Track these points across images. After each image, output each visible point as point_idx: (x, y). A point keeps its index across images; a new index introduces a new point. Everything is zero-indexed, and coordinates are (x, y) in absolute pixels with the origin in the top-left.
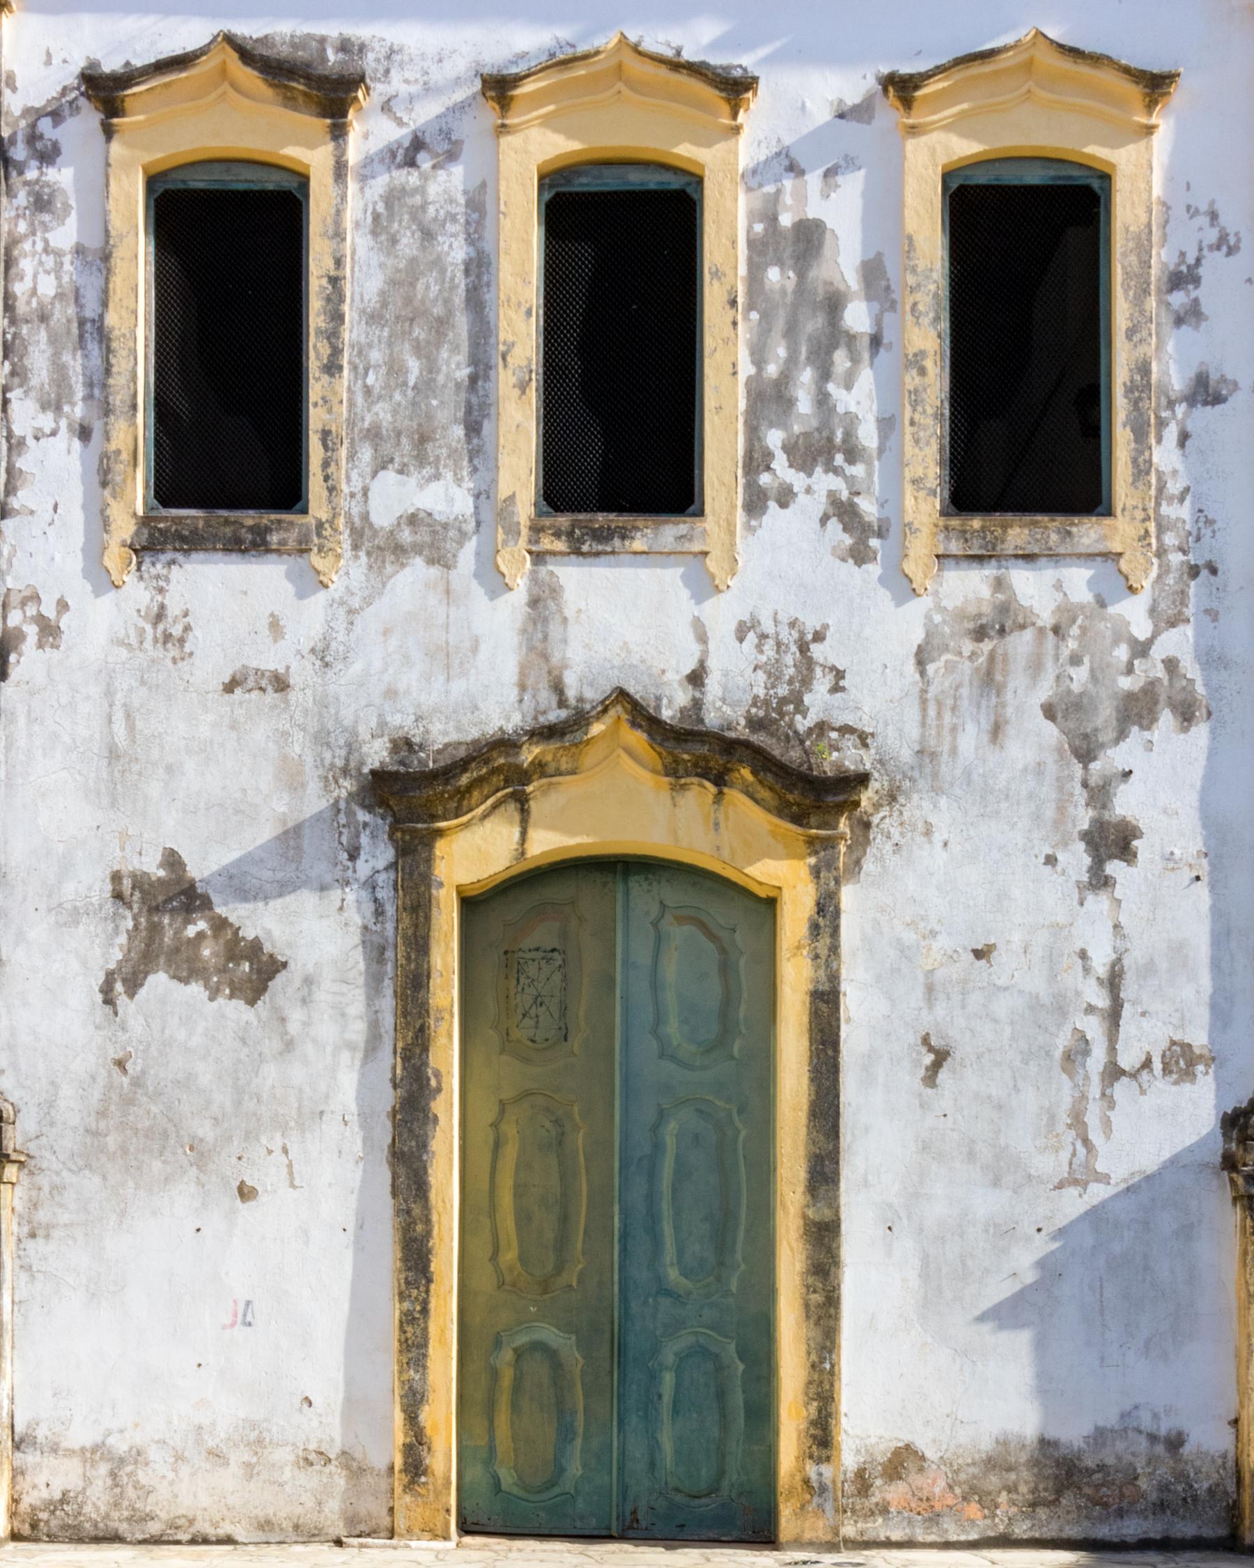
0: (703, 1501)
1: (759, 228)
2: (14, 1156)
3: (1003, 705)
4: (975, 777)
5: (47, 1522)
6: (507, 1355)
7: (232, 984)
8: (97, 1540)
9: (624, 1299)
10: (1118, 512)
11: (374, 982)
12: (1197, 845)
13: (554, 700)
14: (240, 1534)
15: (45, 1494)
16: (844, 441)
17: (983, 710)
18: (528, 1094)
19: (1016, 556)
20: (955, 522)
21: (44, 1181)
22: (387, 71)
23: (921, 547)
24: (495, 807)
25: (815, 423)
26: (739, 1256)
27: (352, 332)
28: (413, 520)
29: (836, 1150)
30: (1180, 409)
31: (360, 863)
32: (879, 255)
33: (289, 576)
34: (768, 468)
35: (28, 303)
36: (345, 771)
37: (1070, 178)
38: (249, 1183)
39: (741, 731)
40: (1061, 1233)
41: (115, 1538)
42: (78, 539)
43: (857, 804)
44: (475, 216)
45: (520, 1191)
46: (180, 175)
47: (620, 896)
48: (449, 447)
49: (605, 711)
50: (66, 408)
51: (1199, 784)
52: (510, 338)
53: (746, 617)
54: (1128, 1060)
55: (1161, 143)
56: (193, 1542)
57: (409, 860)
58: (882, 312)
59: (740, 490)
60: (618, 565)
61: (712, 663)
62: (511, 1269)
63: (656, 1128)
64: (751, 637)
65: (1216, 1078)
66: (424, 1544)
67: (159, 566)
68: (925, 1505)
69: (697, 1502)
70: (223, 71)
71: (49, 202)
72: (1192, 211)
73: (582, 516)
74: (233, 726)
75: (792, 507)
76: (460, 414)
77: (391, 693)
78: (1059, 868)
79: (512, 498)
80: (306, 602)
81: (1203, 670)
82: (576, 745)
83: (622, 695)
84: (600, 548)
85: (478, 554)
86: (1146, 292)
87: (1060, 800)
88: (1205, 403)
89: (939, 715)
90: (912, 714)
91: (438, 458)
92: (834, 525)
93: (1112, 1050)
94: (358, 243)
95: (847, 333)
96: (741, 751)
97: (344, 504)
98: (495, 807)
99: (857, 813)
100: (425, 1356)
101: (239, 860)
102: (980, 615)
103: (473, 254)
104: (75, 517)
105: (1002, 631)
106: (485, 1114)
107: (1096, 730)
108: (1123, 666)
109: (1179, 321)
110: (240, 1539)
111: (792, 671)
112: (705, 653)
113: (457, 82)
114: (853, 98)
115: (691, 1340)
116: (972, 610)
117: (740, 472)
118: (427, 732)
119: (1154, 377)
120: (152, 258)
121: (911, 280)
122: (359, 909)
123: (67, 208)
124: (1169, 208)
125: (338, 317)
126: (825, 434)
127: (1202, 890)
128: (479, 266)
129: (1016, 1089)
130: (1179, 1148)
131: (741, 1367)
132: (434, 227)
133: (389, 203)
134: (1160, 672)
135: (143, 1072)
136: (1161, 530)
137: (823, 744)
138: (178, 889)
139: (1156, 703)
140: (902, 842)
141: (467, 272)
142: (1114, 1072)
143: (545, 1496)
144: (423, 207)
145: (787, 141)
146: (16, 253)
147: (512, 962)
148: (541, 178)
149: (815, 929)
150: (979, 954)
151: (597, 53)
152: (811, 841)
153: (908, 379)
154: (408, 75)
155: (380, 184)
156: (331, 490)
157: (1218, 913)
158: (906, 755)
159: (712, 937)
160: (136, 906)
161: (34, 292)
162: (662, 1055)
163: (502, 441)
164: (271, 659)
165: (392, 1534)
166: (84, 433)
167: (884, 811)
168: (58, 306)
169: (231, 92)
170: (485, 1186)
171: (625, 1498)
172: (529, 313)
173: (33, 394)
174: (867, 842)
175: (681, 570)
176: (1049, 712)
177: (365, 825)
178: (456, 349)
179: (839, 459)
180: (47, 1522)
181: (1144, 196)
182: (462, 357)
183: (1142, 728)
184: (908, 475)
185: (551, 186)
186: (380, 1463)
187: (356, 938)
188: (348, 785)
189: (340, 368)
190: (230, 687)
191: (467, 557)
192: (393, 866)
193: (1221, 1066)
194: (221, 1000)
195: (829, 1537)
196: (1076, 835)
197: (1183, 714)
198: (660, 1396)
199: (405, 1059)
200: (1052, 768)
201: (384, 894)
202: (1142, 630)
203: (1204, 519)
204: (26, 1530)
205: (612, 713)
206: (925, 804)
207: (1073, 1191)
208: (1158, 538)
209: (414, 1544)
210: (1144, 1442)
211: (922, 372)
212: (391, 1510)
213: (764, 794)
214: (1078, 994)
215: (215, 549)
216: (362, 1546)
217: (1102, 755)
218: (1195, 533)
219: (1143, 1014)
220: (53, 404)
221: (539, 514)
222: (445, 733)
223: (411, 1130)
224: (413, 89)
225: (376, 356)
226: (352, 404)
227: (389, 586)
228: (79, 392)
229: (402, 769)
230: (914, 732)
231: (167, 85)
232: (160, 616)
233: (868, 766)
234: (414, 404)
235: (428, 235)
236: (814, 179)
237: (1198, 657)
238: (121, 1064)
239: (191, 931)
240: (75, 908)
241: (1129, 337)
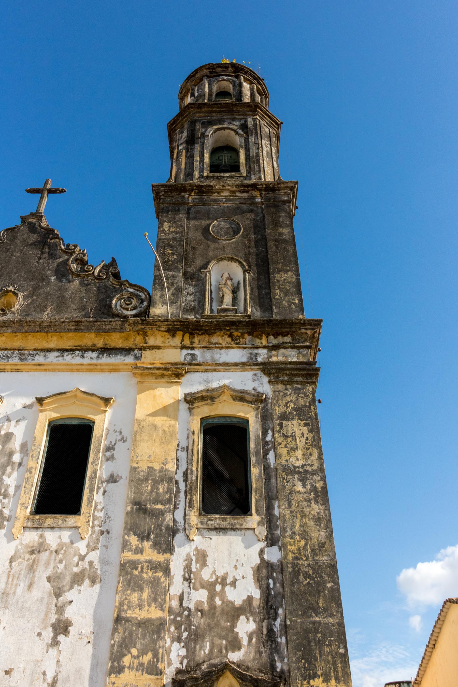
4: (20, 602)
17: (27, 579)
51: (94, 606)
72: (115, 431)
81: (100, 565)
87: (47, 611)
108: (75, 564)
124: (109, 430)
127: (90, 646)
134: (87, 566)
136: (94, 519)
139: (84, 576)
176: (49, 579)
181: (102, 427)
183: (79, 585)
197: (92, 580)
200: (46, 599)
202: (83, 551)
203: (107, 516)
208: (93, 522)
217: (63, 595)
218: (104, 521)
237: (99, 561)
241: (92, 464)
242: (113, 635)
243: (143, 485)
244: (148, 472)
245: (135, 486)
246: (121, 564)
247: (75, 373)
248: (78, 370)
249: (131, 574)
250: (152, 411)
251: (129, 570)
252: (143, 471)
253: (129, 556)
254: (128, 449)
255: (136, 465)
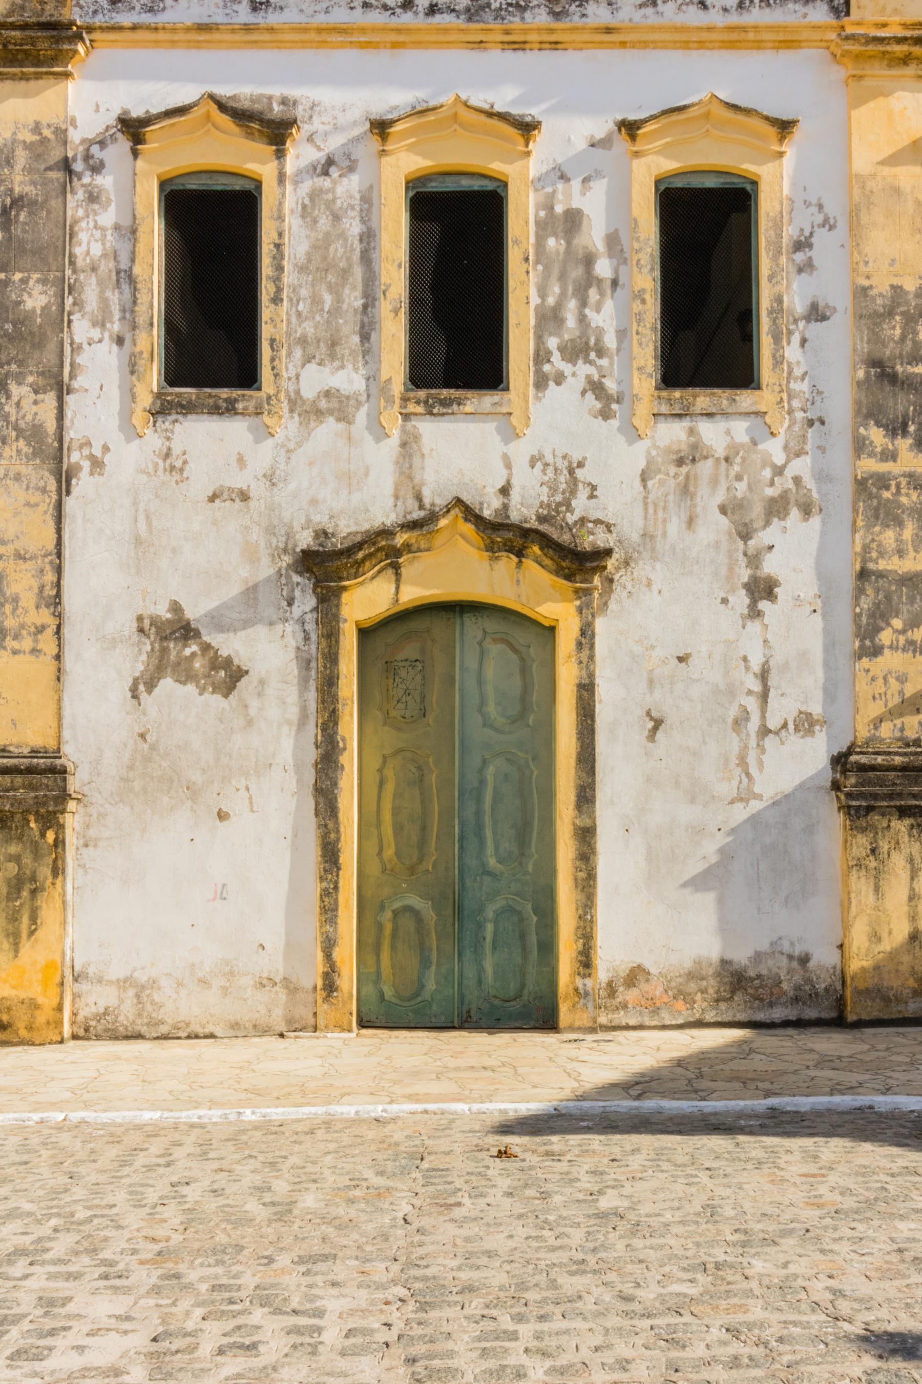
0: (512, 1003)
1: (542, 214)
2: (74, 796)
3: (695, 506)
5: (95, 1027)
6: (388, 914)
7: (213, 684)
8: (127, 1038)
9: (462, 877)
10: (764, 387)
11: (304, 682)
12: (816, 590)
13: (416, 505)
14: (218, 1032)
15: (94, 1009)
16: (596, 344)
18: (400, 751)
19: (702, 414)
20: (664, 394)
21: (93, 810)
22: (311, 117)
23: (644, 409)
24: (379, 572)
25: (577, 333)
26: (533, 850)
27: (289, 277)
28: (327, 394)
29: (594, 782)
30: (802, 324)
31: (294, 608)
32: (616, 230)
33: (249, 429)
34: (549, 361)
35: (84, 260)
36: (285, 551)
37: (733, 183)
38: (224, 809)
39: (533, 524)
40: (733, 831)
41: (139, 1036)
42: (116, 406)
43: (605, 568)
44: (366, 206)
45: (396, 811)
46: (181, 181)
47: (458, 627)
48: (350, 349)
49: (448, 511)
50: (108, 325)
51: (815, 553)
52: (388, 282)
53: (536, 453)
54: (773, 723)
55: (788, 162)
56: (189, 1037)
57: (325, 605)
58: (618, 265)
59: (532, 374)
60: (456, 421)
61: (515, 482)
62: (390, 861)
63: (481, 771)
64: (539, 465)
65: (827, 734)
66: (336, 1035)
67: (167, 423)
68: (650, 1002)
69: (508, 1004)
70: (208, 116)
71: (98, 197)
73: (433, 391)
74: (214, 523)
75: (564, 385)
76: (357, 329)
77: (314, 502)
78: (730, 606)
79: (390, 380)
80: (260, 445)
82: (430, 533)
83: (459, 501)
84: (445, 411)
85: (368, 415)
86: (780, 253)
88: (817, 320)
89: (655, 512)
90: (639, 511)
91: (343, 356)
92: (590, 396)
93: (763, 717)
94: (293, 223)
95: (597, 278)
96: (533, 536)
97: (284, 384)
98: (379, 572)
99: (605, 573)
100: (336, 916)
101: (218, 607)
102: (680, 451)
103: (365, 230)
104: (114, 393)
105: (694, 460)
106: (374, 763)
107: (752, 520)
108: (768, 481)
109: (800, 270)
110: (218, 1035)
111: (564, 486)
112: (510, 475)
113: (355, 123)
114: (600, 135)
115: (504, 903)
116: (675, 448)
117: (531, 363)
118: (337, 525)
119: (785, 305)
120: (163, 232)
121: (636, 245)
122: (294, 637)
123: (109, 201)
125: (280, 269)
126: (584, 340)
127: (817, 617)
128: (369, 237)
129: (704, 742)
130: (805, 778)
131: (535, 919)
132: (340, 213)
133: (312, 199)
134: (790, 485)
135: (157, 741)
136: (790, 398)
137: (584, 531)
138: (179, 625)
139: (788, 504)
140: (633, 590)
141: (361, 240)
142: (765, 731)
143: (413, 1003)
144: (334, 201)
145: (560, 160)
146: (76, 229)
147: (390, 669)
148: (407, 183)
149: (580, 645)
150: (681, 659)
151: (442, 106)
152: (577, 591)
153: (634, 306)
154: (323, 119)
155: (306, 186)
156: (276, 375)
157: (827, 632)
158: (635, 537)
159: (516, 651)
160: (152, 637)
161: (88, 253)
162: (484, 725)
163: (383, 345)
164: (238, 481)
165: (315, 1029)
166: (120, 341)
167: (622, 572)
168: (103, 262)
169: (213, 130)
170: (374, 809)
171: (462, 1003)
172: (400, 266)
173: (87, 317)
174: (611, 591)
175: (495, 424)
176: (723, 510)
177: (298, 584)
178: (354, 288)
179: (593, 355)
180: (95, 1027)
182: (358, 293)
183: (780, 519)
184: (635, 365)
185: (413, 188)
186: (308, 985)
187: (292, 655)
188: (287, 559)
189: (282, 300)
190: (212, 499)
191: (361, 416)
192: (316, 609)
193: (830, 726)
194: (206, 695)
195: (590, 1024)
196: (740, 586)
197: (805, 510)
198: (484, 939)
199: (323, 730)
201: (311, 627)
202: (779, 458)
204: (81, 1033)
205: (453, 512)
206: (646, 567)
207: (740, 805)
208: (789, 403)
209: (329, 1035)
210: (784, 961)
211: (643, 302)
212: (315, 1014)
213: (548, 562)
214: (742, 683)
215: (202, 413)
216: (296, 1037)
217: (755, 536)
219: (782, 695)
220: (100, 323)
221: (407, 390)
222: (348, 526)
223: (327, 775)
224: (327, 128)
225: (304, 292)
226: (289, 322)
227: (313, 435)
228: (117, 315)
229: (321, 549)
230: (639, 522)
231: (172, 125)
232: (168, 455)
233: (612, 544)
234: (328, 322)
235: (336, 218)
236: (576, 184)
237: (813, 476)
238: (142, 736)
239: (187, 652)
240: (114, 639)
242: (857, 599)
243: (885, 326)
244: (892, 297)
245: (868, 328)
246: (856, 479)
247: (695, 54)
248: (701, 45)
249: (879, 498)
250: (888, 151)
251: (874, 490)
252: (881, 295)
253: (870, 465)
254: (842, 246)
255: (866, 283)
